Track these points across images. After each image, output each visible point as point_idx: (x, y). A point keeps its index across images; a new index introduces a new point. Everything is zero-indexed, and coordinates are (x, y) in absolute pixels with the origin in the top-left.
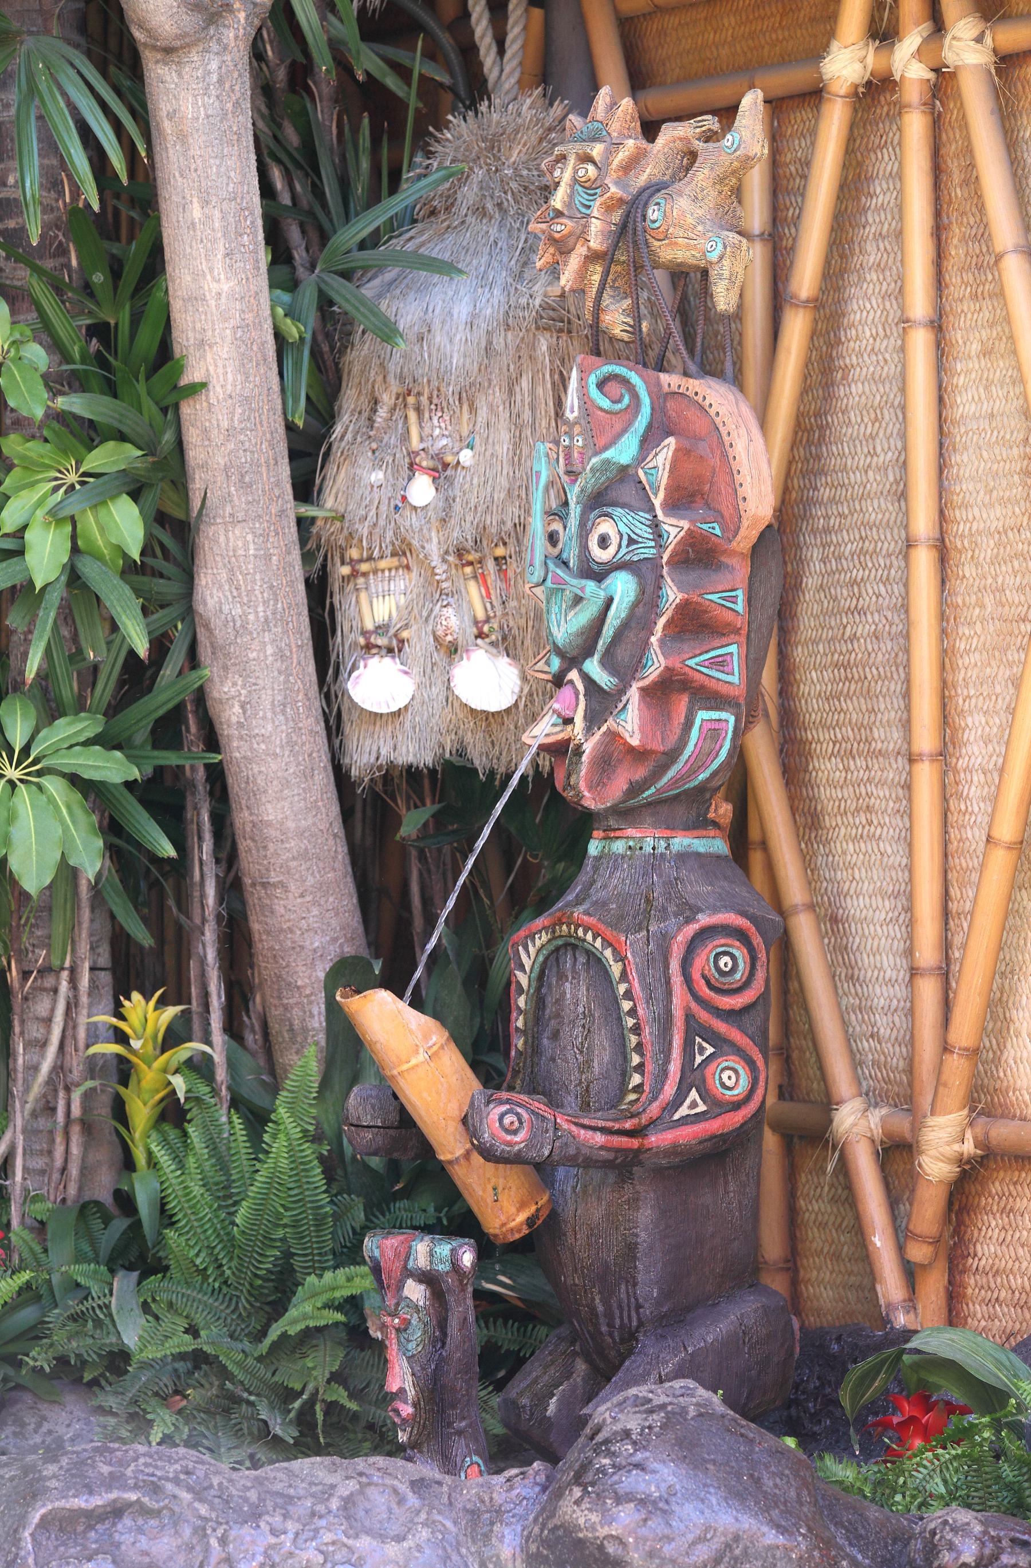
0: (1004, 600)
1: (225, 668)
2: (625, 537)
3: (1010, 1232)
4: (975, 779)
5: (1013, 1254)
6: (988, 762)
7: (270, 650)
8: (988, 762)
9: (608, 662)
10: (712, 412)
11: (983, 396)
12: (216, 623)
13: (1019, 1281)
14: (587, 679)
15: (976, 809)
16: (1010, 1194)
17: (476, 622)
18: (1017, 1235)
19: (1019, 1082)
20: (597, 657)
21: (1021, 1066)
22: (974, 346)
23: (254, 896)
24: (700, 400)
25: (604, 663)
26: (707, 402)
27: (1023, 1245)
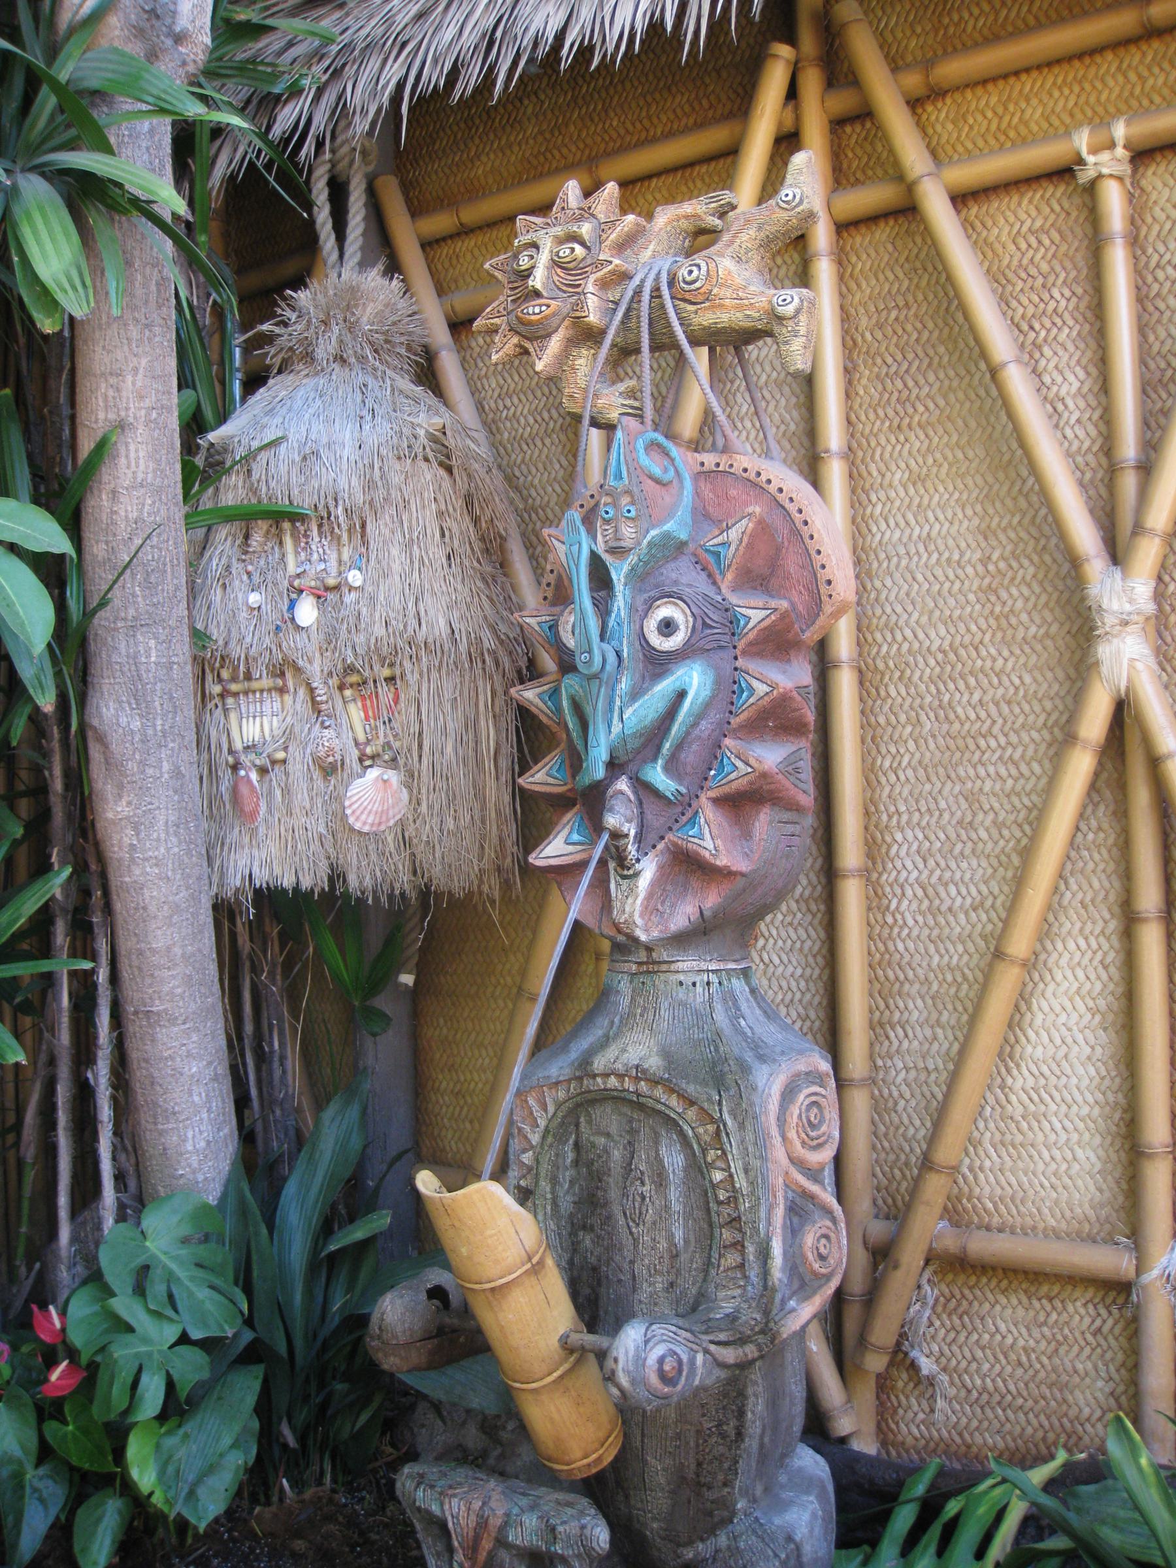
0: (952, 716)
1: (121, 786)
2: (699, 621)
3: (964, 1334)
4: (909, 892)
5: (968, 1355)
6: (929, 877)
7: (166, 766)
8: (929, 877)
9: (672, 767)
10: (772, 488)
11: (913, 522)
12: (114, 739)
13: (978, 1382)
14: (643, 787)
15: (910, 922)
16: (963, 1296)
17: (357, 744)
18: (975, 1336)
19: (977, 1191)
20: (660, 762)
21: (981, 1176)
22: (898, 475)
23: (134, 1028)
24: (752, 476)
25: (667, 769)
26: (764, 478)
27: (983, 1348)
